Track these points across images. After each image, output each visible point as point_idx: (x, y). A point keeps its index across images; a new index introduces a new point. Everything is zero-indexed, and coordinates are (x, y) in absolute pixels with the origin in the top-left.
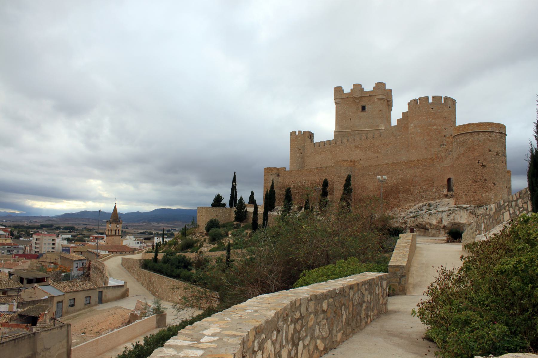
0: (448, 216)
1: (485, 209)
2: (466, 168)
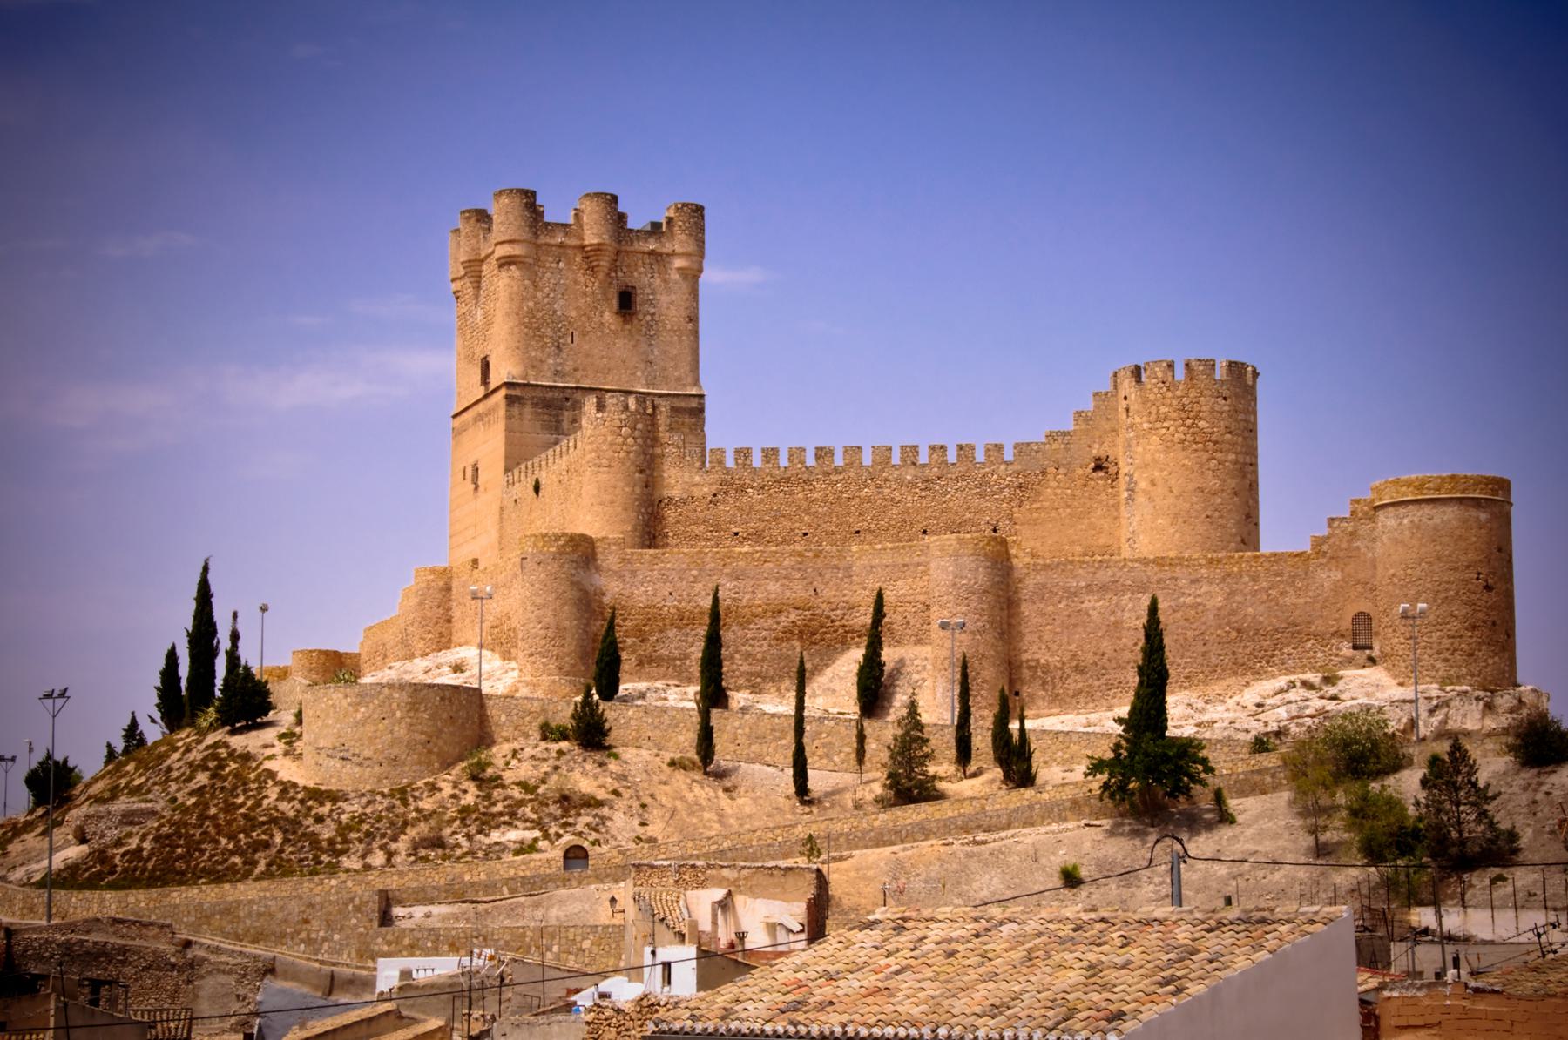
2: (1447, 590)
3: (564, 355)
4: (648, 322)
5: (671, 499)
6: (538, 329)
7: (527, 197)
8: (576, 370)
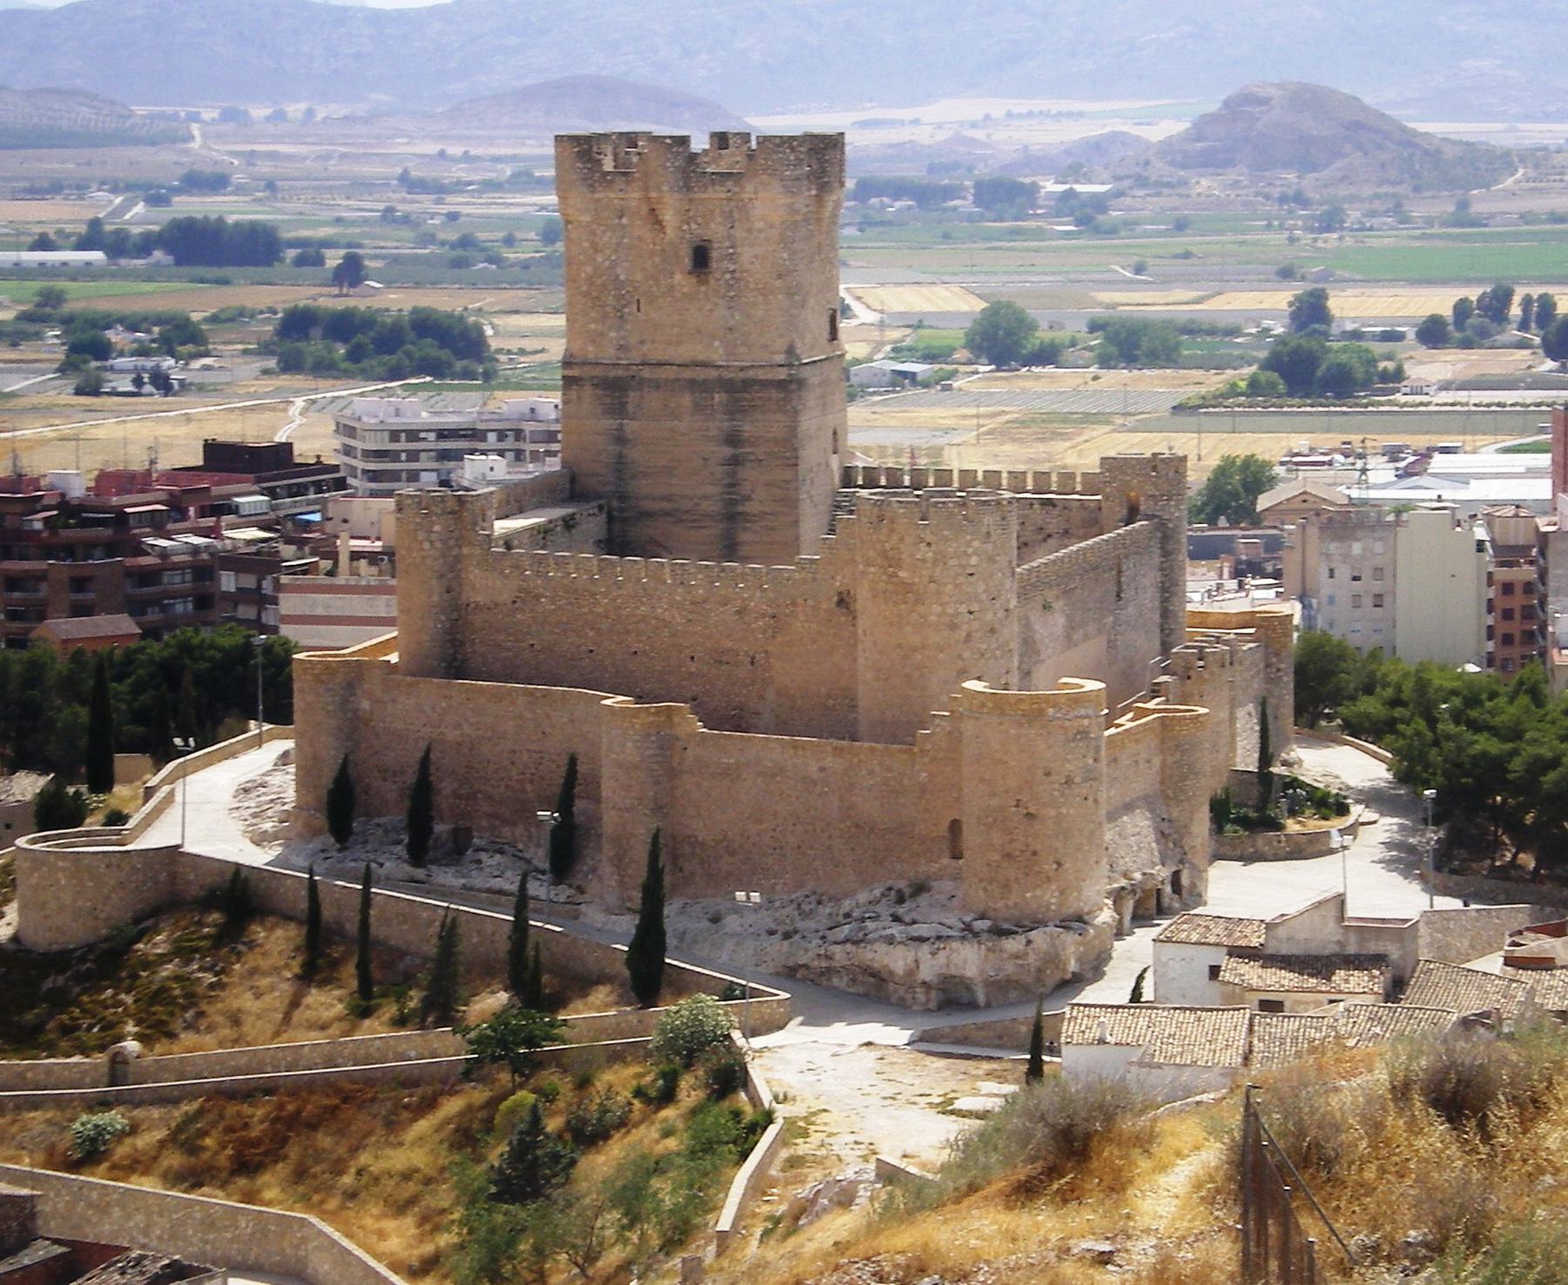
0: (933, 954)
1: (1024, 941)
3: (629, 327)
5: (477, 604)
7: (579, 145)
8: (642, 342)
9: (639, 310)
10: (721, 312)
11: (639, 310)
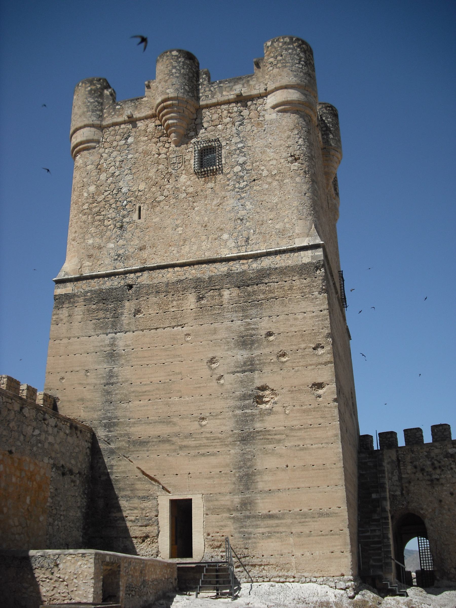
4: (236, 174)
6: (98, 213)
9: (140, 218)
10: (231, 202)
11: (140, 218)
